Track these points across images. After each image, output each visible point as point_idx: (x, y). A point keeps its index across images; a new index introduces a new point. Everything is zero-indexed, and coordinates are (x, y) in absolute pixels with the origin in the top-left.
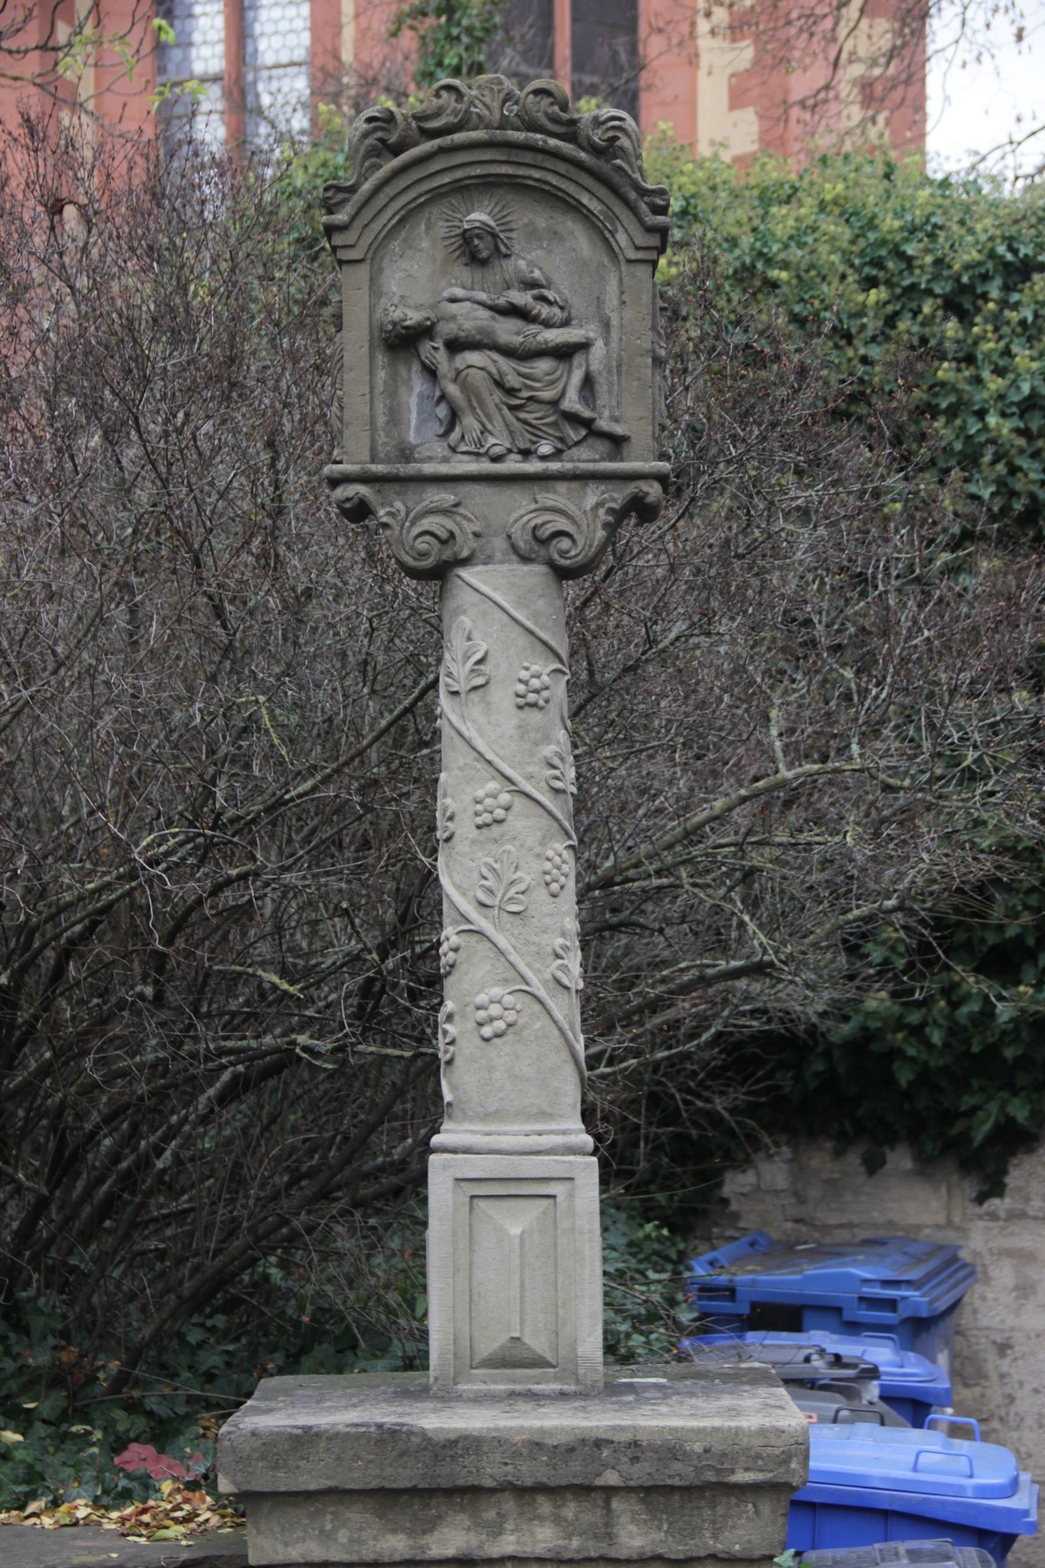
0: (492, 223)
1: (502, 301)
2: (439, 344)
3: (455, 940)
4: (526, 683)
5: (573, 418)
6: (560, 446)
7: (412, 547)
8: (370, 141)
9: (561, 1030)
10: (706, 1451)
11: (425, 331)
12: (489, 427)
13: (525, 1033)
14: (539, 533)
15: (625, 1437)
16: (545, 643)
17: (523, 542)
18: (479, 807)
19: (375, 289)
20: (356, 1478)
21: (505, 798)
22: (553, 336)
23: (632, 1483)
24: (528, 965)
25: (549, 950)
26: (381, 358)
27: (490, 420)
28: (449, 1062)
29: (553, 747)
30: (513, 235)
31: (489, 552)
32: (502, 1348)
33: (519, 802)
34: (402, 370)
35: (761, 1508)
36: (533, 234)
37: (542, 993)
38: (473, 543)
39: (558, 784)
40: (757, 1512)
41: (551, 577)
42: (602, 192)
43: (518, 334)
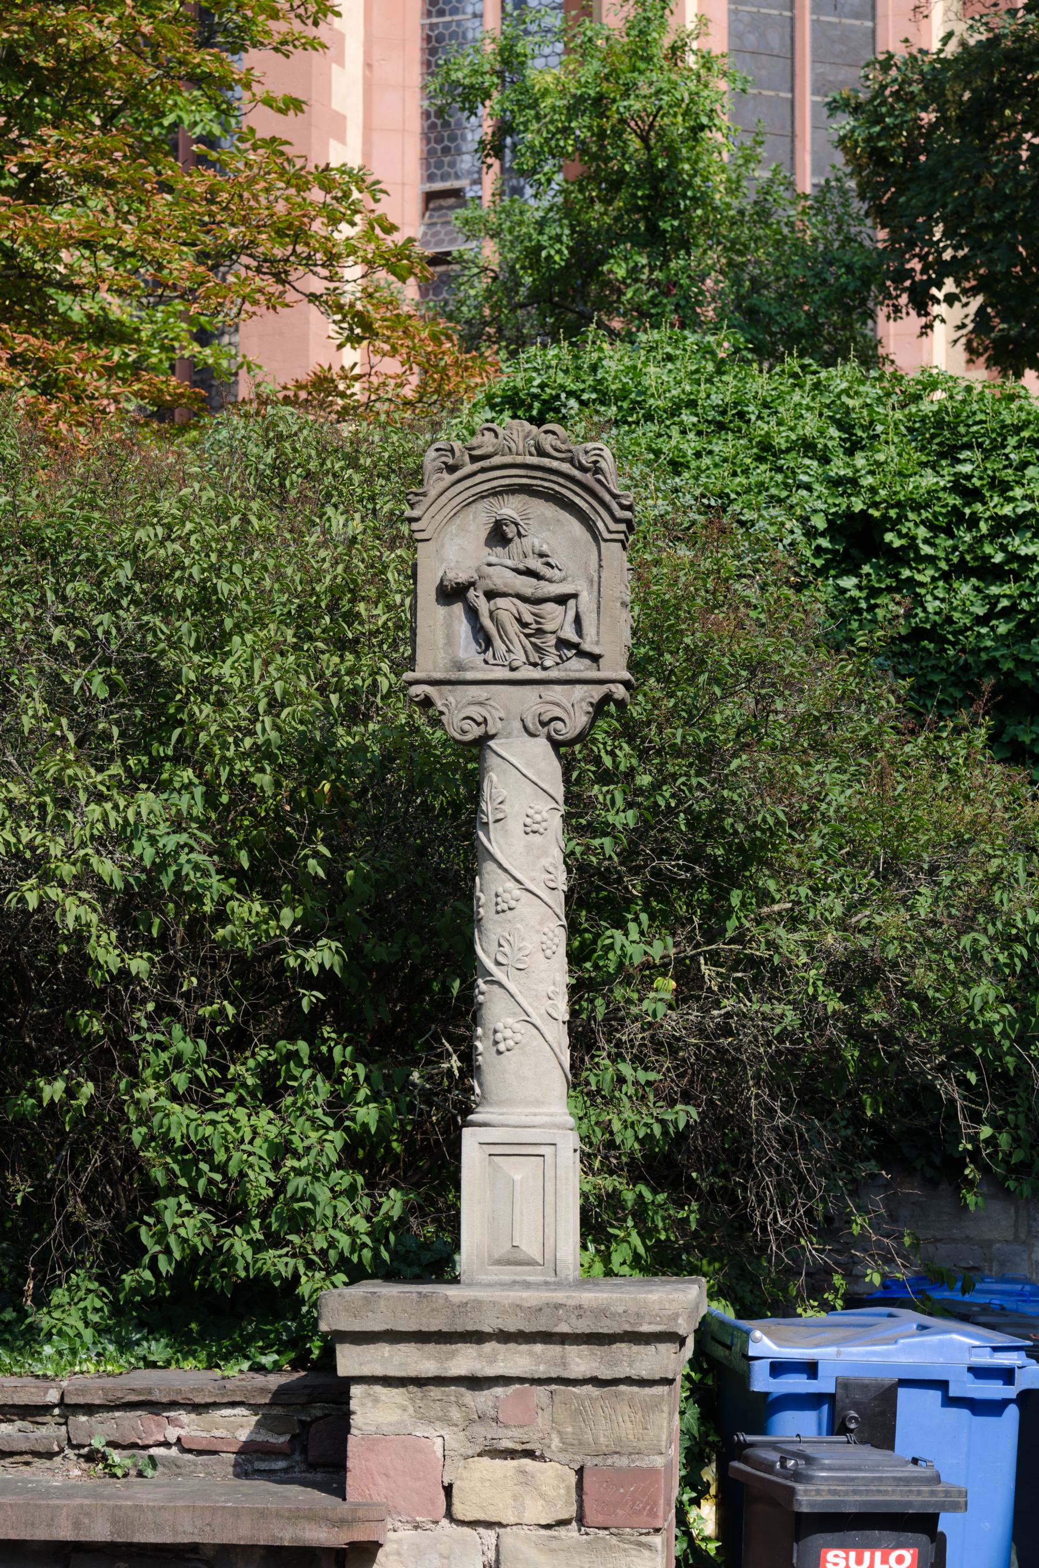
1: (521, 566)
21: (517, 893)
36: (544, 522)
39: (552, 885)
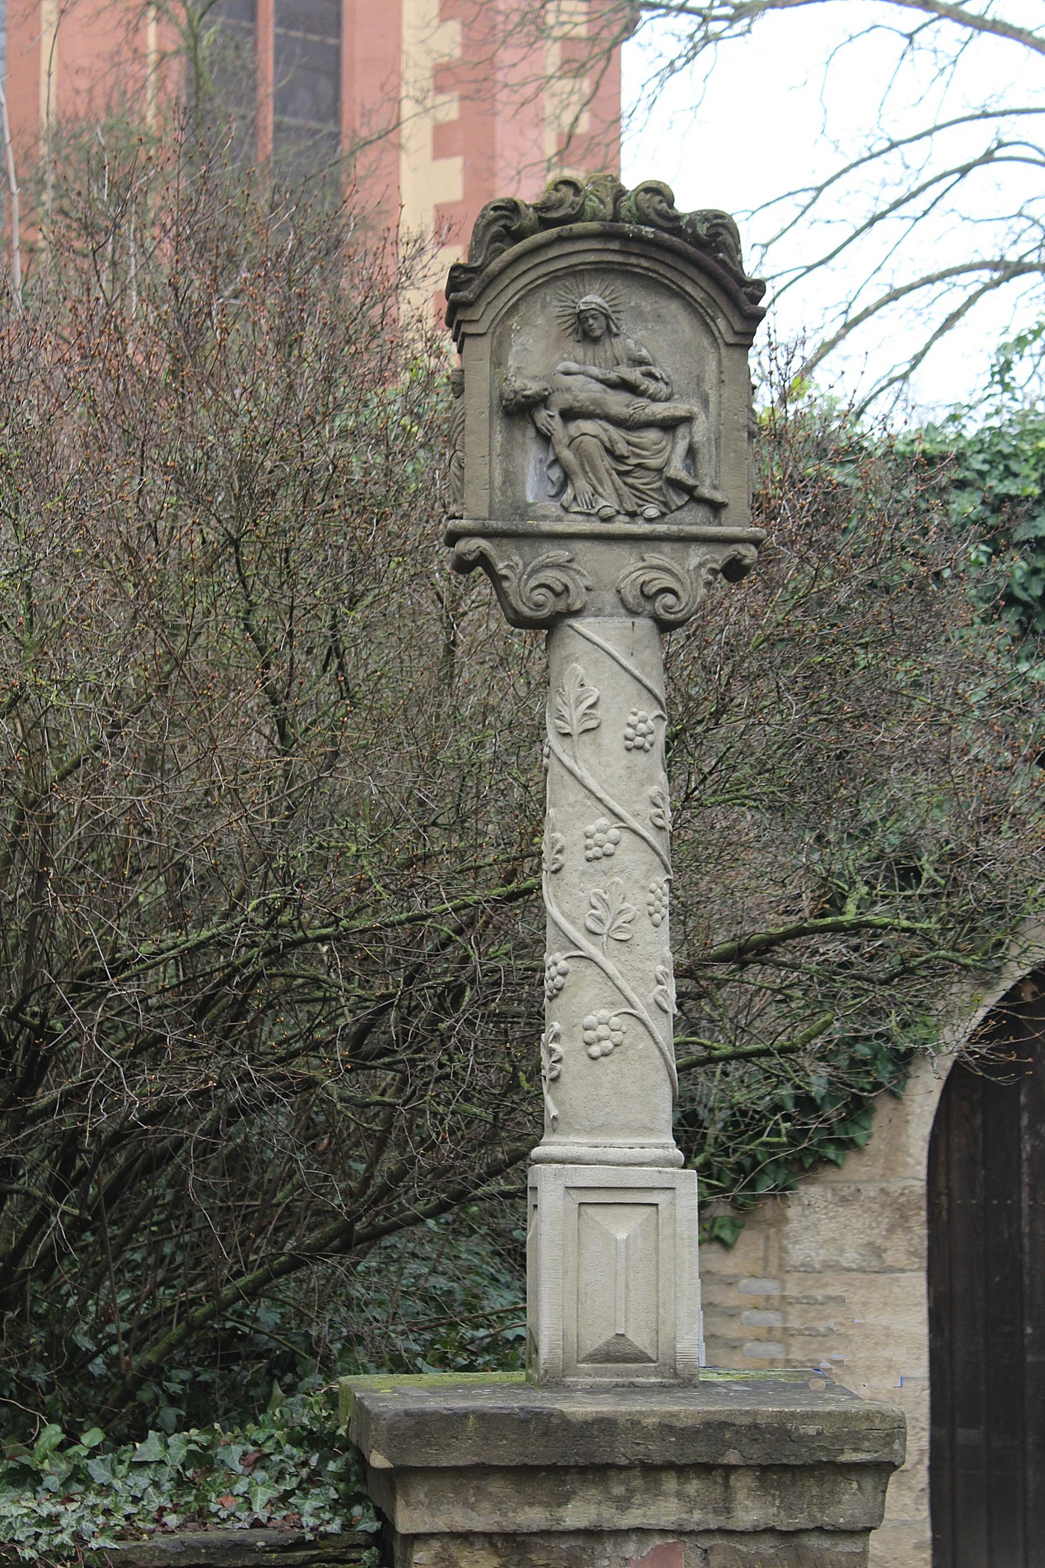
0: (606, 305)
1: (613, 376)
2: (555, 412)
3: (563, 965)
4: (634, 727)
5: (675, 484)
6: (664, 510)
7: (528, 599)
8: (495, 228)
9: (660, 1050)
10: (818, 1434)
11: (541, 401)
12: (601, 490)
13: (630, 1052)
14: (646, 589)
15: (747, 1421)
16: (650, 691)
17: (631, 595)
18: (590, 841)
19: (498, 362)
20: (505, 1454)
21: (614, 833)
22: (660, 410)
23: (752, 1462)
24: (633, 989)
25: (652, 975)
26: (498, 425)
27: (601, 484)
28: (555, 1080)
29: (656, 788)
30: (621, 316)
31: (600, 605)
32: (608, 1343)
33: (626, 838)
34: (518, 435)
35: (864, 1485)
36: (639, 315)
37: (645, 1016)
38: (585, 597)
39: (660, 822)
40: (860, 1488)
41: (655, 630)
42: (703, 281)
43: (628, 406)
